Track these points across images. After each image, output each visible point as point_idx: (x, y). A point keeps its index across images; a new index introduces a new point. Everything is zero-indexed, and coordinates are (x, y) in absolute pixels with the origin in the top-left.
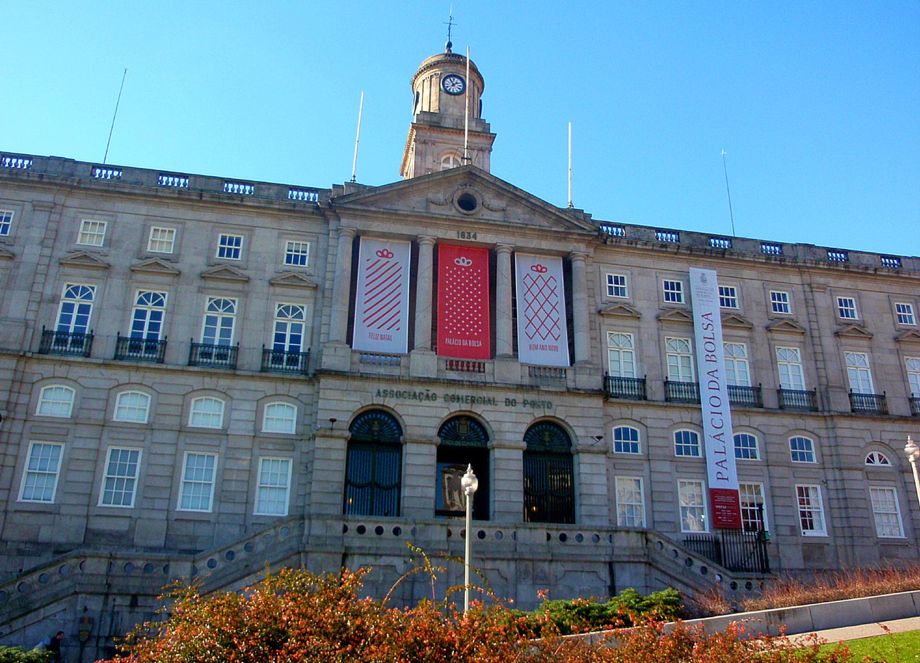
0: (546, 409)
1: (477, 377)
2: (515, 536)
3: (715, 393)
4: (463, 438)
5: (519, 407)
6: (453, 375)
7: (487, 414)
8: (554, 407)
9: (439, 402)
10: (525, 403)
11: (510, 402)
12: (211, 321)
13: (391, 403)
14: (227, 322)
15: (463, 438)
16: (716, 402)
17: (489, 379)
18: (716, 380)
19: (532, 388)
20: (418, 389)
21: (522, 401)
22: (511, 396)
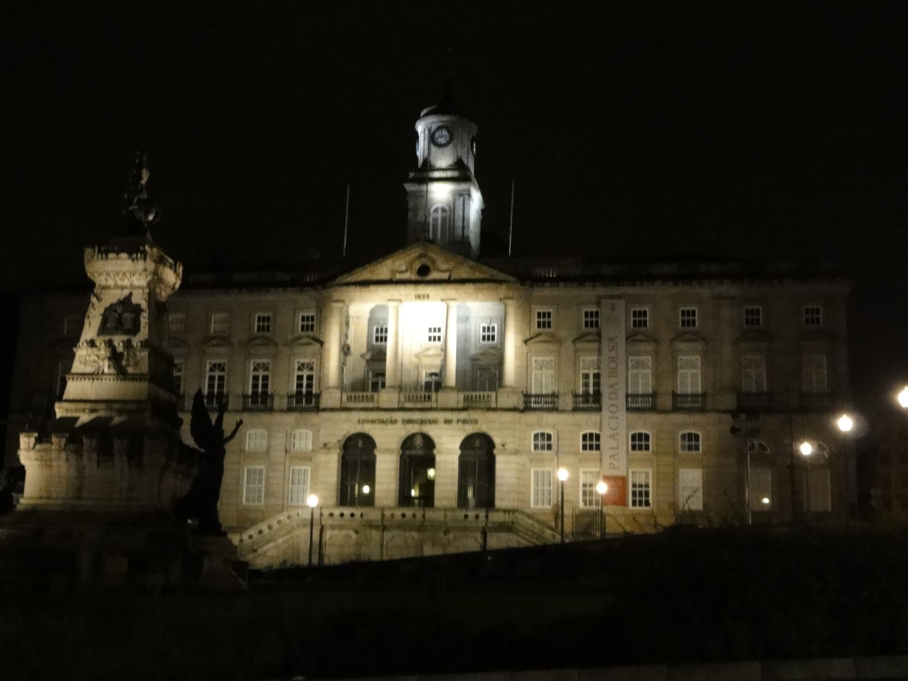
0: (473, 425)
1: (427, 405)
2: (424, 516)
3: (614, 402)
4: (418, 448)
5: (454, 425)
6: (408, 405)
7: (433, 431)
8: (479, 423)
9: (399, 424)
10: (458, 421)
11: (448, 422)
12: (256, 378)
13: (367, 429)
14: (265, 378)
15: (418, 448)
16: (613, 409)
17: (434, 405)
18: (616, 391)
19: (464, 409)
20: (385, 416)
21: (456, 420)
22: (449, 415)
